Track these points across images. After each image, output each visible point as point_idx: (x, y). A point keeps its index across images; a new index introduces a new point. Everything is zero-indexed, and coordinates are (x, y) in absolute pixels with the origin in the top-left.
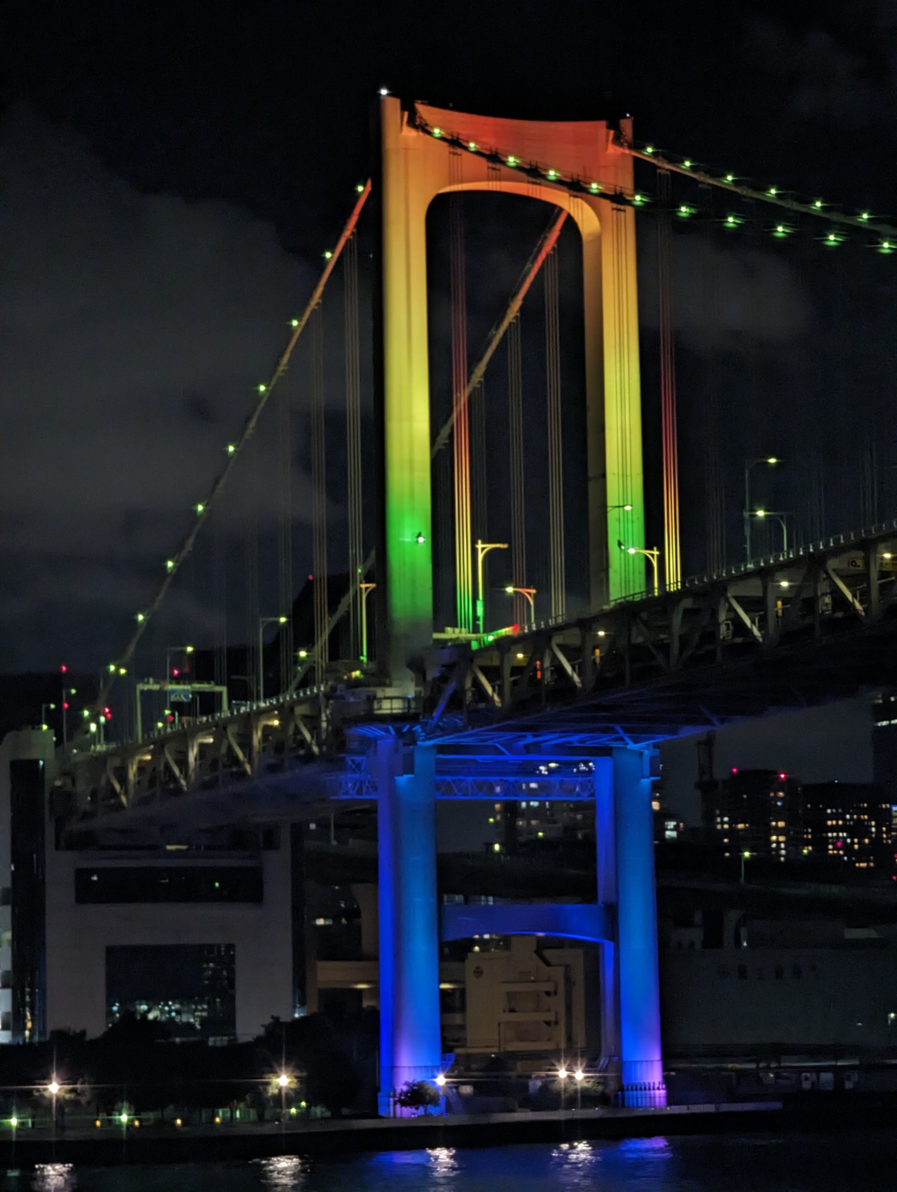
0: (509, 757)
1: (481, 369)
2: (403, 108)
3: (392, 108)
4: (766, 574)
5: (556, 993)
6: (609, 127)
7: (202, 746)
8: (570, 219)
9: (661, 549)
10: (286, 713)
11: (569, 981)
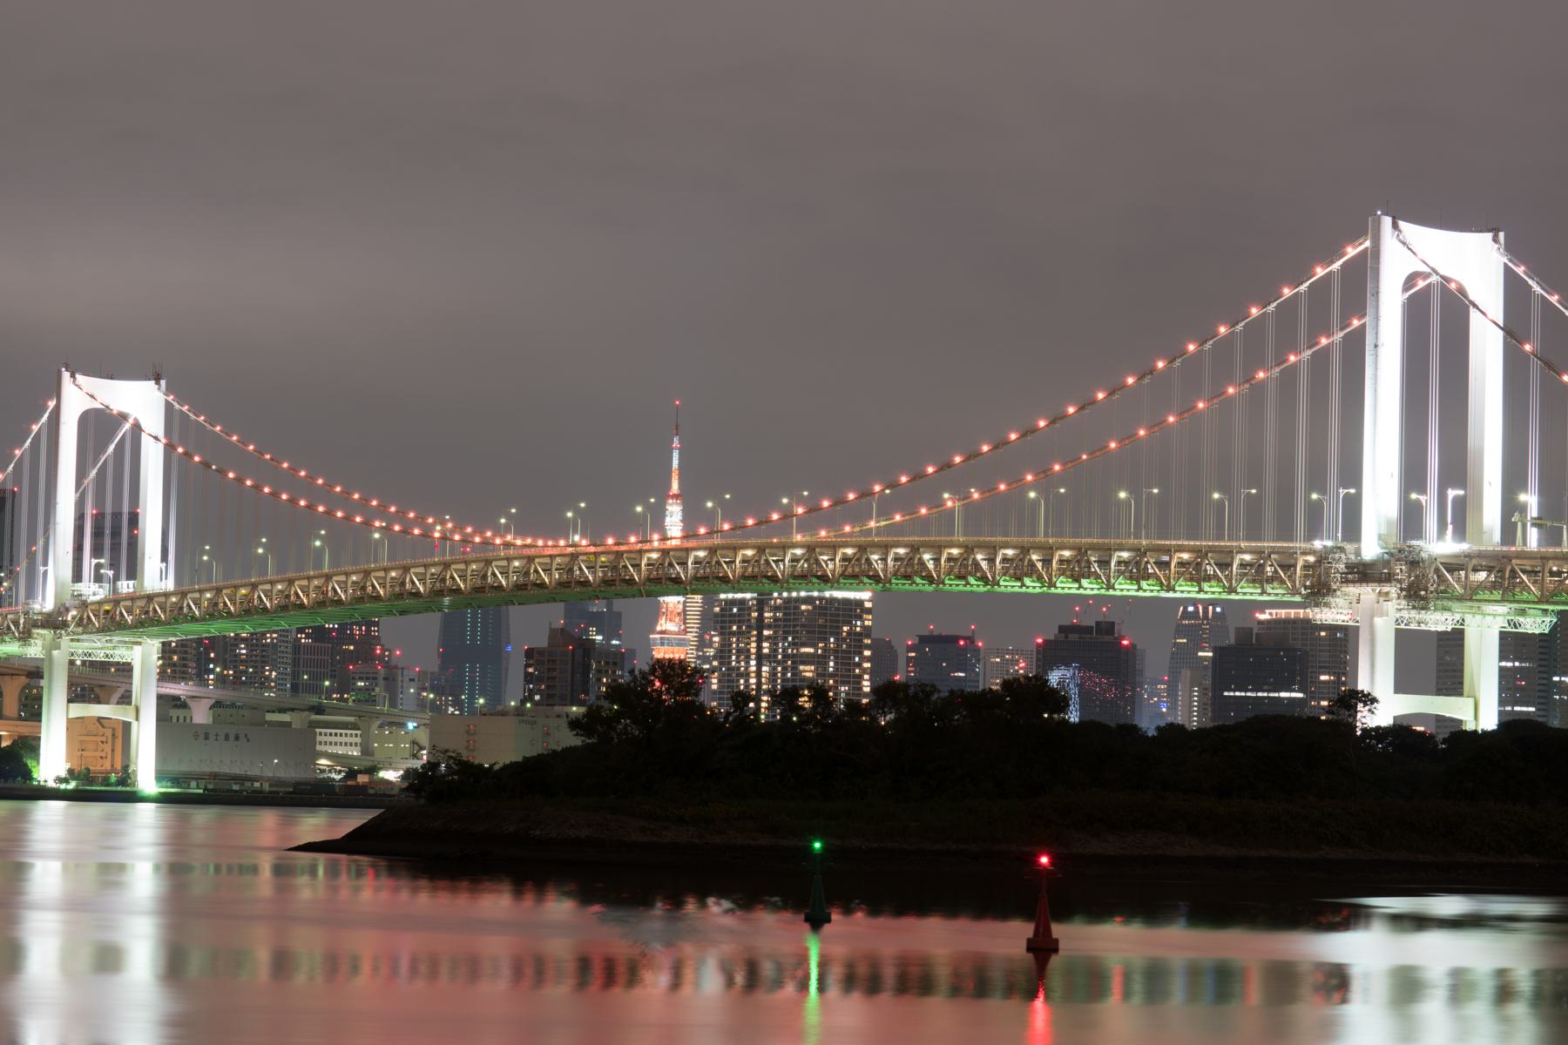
0: (99, 645)
1: (94, 472)
2: (71, 377)
3: (66, 375)
4: (201, 591)
5: (107, 742)
6: (156, 384)
8: (136, 419)
9: (167, 563)
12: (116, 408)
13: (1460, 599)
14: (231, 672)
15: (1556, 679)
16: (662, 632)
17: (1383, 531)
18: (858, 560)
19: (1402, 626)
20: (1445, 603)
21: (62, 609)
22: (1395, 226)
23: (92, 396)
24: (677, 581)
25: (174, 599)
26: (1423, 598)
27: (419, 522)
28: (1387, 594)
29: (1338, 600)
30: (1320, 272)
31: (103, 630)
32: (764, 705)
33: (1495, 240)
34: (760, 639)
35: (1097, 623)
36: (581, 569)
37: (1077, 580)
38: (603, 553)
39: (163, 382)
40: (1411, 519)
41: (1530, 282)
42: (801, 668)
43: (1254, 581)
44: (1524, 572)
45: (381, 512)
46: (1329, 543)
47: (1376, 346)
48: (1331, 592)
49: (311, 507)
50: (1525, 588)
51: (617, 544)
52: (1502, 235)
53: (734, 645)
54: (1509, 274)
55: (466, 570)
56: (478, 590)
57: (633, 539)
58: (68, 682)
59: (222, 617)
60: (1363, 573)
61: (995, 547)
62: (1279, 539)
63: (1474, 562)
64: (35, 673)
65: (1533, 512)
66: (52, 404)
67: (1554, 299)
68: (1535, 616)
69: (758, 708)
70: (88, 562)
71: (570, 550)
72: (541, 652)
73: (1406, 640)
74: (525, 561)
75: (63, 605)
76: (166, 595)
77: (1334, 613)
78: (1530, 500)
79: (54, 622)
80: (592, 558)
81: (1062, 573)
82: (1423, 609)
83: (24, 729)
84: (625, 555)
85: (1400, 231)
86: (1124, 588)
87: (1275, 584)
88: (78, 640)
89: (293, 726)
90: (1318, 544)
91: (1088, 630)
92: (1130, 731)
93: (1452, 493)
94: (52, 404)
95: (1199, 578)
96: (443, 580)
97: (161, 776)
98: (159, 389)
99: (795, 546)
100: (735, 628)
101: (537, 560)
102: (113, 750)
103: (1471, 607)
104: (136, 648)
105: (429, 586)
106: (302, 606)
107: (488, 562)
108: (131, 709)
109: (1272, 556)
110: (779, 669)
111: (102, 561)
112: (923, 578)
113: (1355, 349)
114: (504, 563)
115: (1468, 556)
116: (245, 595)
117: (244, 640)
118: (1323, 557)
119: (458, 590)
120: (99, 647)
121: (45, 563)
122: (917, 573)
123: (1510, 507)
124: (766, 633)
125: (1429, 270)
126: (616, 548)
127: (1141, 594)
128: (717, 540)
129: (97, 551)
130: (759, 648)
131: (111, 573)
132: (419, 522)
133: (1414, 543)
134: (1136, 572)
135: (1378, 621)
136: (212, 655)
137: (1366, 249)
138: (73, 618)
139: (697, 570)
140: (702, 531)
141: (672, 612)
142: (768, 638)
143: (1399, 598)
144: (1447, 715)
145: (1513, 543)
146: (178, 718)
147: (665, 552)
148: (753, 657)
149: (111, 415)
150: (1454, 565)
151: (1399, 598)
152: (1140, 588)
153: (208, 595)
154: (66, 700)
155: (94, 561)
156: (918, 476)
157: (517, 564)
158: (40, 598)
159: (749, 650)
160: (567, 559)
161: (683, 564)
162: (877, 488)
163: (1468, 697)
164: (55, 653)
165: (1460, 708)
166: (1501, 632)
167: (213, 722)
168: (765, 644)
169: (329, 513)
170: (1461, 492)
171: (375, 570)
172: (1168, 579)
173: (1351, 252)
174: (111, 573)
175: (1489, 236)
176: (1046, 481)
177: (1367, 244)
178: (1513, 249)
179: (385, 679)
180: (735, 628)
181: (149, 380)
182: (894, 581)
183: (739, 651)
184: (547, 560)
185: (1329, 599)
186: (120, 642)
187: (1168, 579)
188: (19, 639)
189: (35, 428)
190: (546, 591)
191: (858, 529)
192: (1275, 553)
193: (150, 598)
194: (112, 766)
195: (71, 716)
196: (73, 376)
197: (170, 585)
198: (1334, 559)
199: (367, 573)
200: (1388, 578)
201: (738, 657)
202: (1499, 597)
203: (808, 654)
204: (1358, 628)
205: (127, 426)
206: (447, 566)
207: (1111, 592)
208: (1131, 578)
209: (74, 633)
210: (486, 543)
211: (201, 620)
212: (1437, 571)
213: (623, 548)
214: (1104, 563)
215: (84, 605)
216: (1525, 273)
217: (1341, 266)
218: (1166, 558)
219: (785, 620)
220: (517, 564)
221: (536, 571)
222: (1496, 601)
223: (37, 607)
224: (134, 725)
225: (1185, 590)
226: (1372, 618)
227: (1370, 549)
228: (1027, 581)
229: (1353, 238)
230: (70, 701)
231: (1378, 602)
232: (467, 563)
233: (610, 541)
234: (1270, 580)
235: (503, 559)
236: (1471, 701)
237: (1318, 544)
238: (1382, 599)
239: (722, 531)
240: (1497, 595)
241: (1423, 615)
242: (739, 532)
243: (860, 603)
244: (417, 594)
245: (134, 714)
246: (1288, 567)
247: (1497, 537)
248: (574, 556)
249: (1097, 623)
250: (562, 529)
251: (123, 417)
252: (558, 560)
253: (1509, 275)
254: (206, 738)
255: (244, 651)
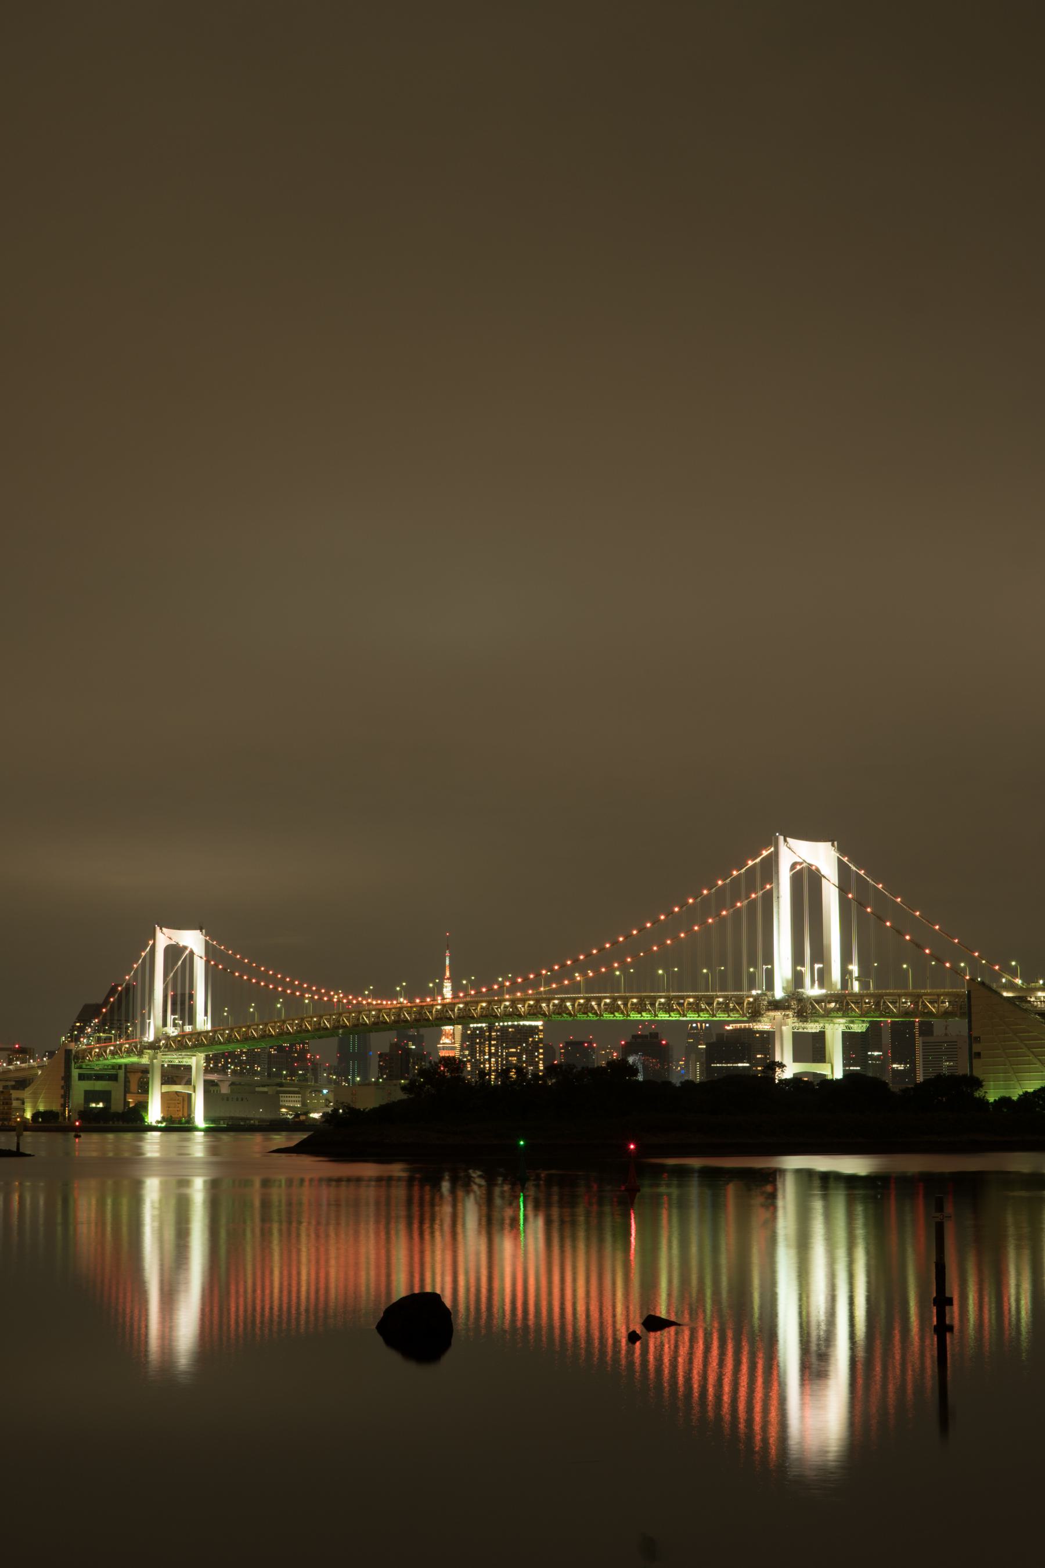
0: (175, 1056)
1: (172, 974)
3: (158, 929)
4: (224, 1030)
7: (110, 1050)
8: (191, 949)
9: (207, 1016)
10: (130, 1045)
11: (183, 1100)
12: (181, 944)
13: (823, 1016)
14: (239, 1068)
15: (870, 1053)
16: (443, 1044)
17: (785, 985)
18: (536, 1006)
19: (796, 1030)
20: (816, 1019)
21: (157, 1040)
22: (785, 841)
23: (170, 938)
24: (450, 1019)
25: (211, 1034)
26: (805, 1017)
27: (327, 994)
28: (788, 1015)
29: (764, 1019)
30: (750, 863)
31: (177, 1050)
32: (493, 1077)
33: (833, 845)
34: (490, 1046)
35: (650, 1033)
36: (404, 1015)
37: (640, 1013)
38: (414, 1006)
39: (204, 931)
40: (798, 979)
41: (850, 865)
42: (510, 1058)
43: (724, 1011)
44: (853, 1002)
45: (309, 990)
46: (759, 992)
47: (778, 897)
48: (761, 1015)
49: (275, 988)
50: (853, 1010)
51: (420, 1002)
52: (836, 843)
53: (478, 1049)
54: (840, 861)
55: (349, 1017)
56: (355, 1026)
57: (428, 1000)
58: (161, 1074)
59: (234, 1042)
60: (776, 1005)
61: (600, 998)
62: (735, 991)
63: (829, 998)
64: (145, 1071)
65: (856, 974)
66: (151, 942)
67: (862, 872)
68: (858, 1023)
69: (490, 1078)
70: (170, 1018)
71: (399, 1005)
72: (386, 1055)
73: (797, 1037)
74: (377, 1011)
75: (158, 1038)
76: (207, 1032)
77: (763, 1025)
78: (854, 968)
79: (154, 1046)
80: (409, 1009)
81: (633, 1009)
82: (805, 1022)
83: (140, 1098)
84: (425, 1008)
85: (788, 843)
86: (663, 1016)
87: (735, 1012)
88: (166, 1055)
89: (269, 1093)
90: (754, 992)
91: (646, 1036)
92: (668, 1084)
93: (817, 966)
94: (151, 942)
95: (698, 1010)
96: (339, 1022)
97: (207, 1118)
98: (202, 934)
99: (506, 1000)
100: (478, 1041)
101: (383, 1011)
102: (183, 1107)
103: (828, 1020)
104: (194, 1058)
105: (332, 1024)
106: (272, 1035)
107: (360, 1013)
108: (191, 1087)
109: (733, 999)
110: (500, 1059)
111: (176, 1017)
112: (567, 1014)
113: (768, 900)
114: (368, 1013)
115: (826, 996)
116: (245, 1031)
117: (244, 1053)
118: (757, 998)
119: (346, 1026)
120: (176, 1059)
121: (149, 1019)
122: (564, 1012)
123: (845, 973)
124: (493, 1042)
125: (801, 861)
126: (421, 1004)
127: (671, 1018)
128: (468, 999)
129: (174, 1012)
130: (490, 1050)
131: (181, 1022)
132: (327, 994)
133: (800, 990)
134: (668, 1009)
135: (784, 1028)
136: (229, 1060)
137: (772, 852)
138: (163, 1044)
139: (459, 1013)
140: (461, 995)
141: (448, 1034)
142: (494, 1045)
143: (793, 1017)
144: (818, 1072)
145: (847, 989)
146: (214, 1091)
147: (444, 1005)
148: (487, 1054)
149: (180, 947)
150: (819, 1000)
151: (793, 1017)
152: (670, 1016)
153: (227, 1032)
154: (160, 1084)
155: (173, 1017)
156: (563, 966)
157: (373, 1013)
158: (147, 1035)
159: (485, 1051)
160: (397, 1010)
161: (453, 1010)
162: (544, 972)
163: (828, 1063)
164: (155, 1061)
165: (824, 1069)
166: (842, 1032)
167: (231, 1092)
168: (493, 1048)
169: (284, 991)
170: (821, 966)
171: (306, 1018)
172: (683, 1011)
173: (765, 853)
174: (181, 1022)
175: (830, 843)
176: (624, 967)
177: (772, 849)
178: (841, 850)
179: (312, 1069)
180: (478, 1041)
181: (197, 930)
182: (553, 1016)
183: (480, 1052)
184: (388, 1011)
185: (762, 1019)
186: (185, 1055)
187: (683, 1011)
188: (137, 1055)
189: (143, 954)
190: (388, 1025)
191: (535, 992)
192: (733, 997)
193: (200, 1034)
194: (183, 1114)
195: (163, 1091)
196: (161, 929)
197: (209, 1027)
198: (762, 999)
199: (302, 1019)
200: (788, 1008)
201: (480, 1054)
202: (841, 1015)
203: (513, 1052)
204: (774, 1031)
205: (187, 952)
206: (340, 1015)
207: (656, 1018)
208: (666, 1011)
209: (164, 1051)
210: (359, 1003)
211: (224, 1043)
212: (811, 1003)
213: (424, 1004)
214: (653, 1005)
215: (168, 1038)
216: (847, 860)
217: (760, 860)
218: (682, 1001)
219: (502, 1036)
220: (373, 1013)
221: (383, 1016)
222: (840, 1017)
223: (145, 1039)
224: (193, 1095)
225: (691, 1016)
226: (781, 1026)
227: (779, 994)
228: (617, 1014)
229: (766, 847)
230: (162, 1084)
231: (783, 1019)
232: (350, 1013)
233: (418, 1001)
234: (732, 1010)
235: (367, 1011)
236: (829, 1065)
237: (754, 992)
238: (785, 1018)
239: (470, 994)
240: (840, 1014)
241: (805, 1025)
242: (479, 995)
243: (537, 1027)
244: (327, 1028)
245: (192, 1089)
246: (740, 1004)
247: (839, 986)
248: (401, 1009)
249: (650, 1033)
250: (395, 996)
251: (185, 948)
252: (394, 1010)
253: (841, 865)
254: (228, 1099)
255: (245, 1058)
